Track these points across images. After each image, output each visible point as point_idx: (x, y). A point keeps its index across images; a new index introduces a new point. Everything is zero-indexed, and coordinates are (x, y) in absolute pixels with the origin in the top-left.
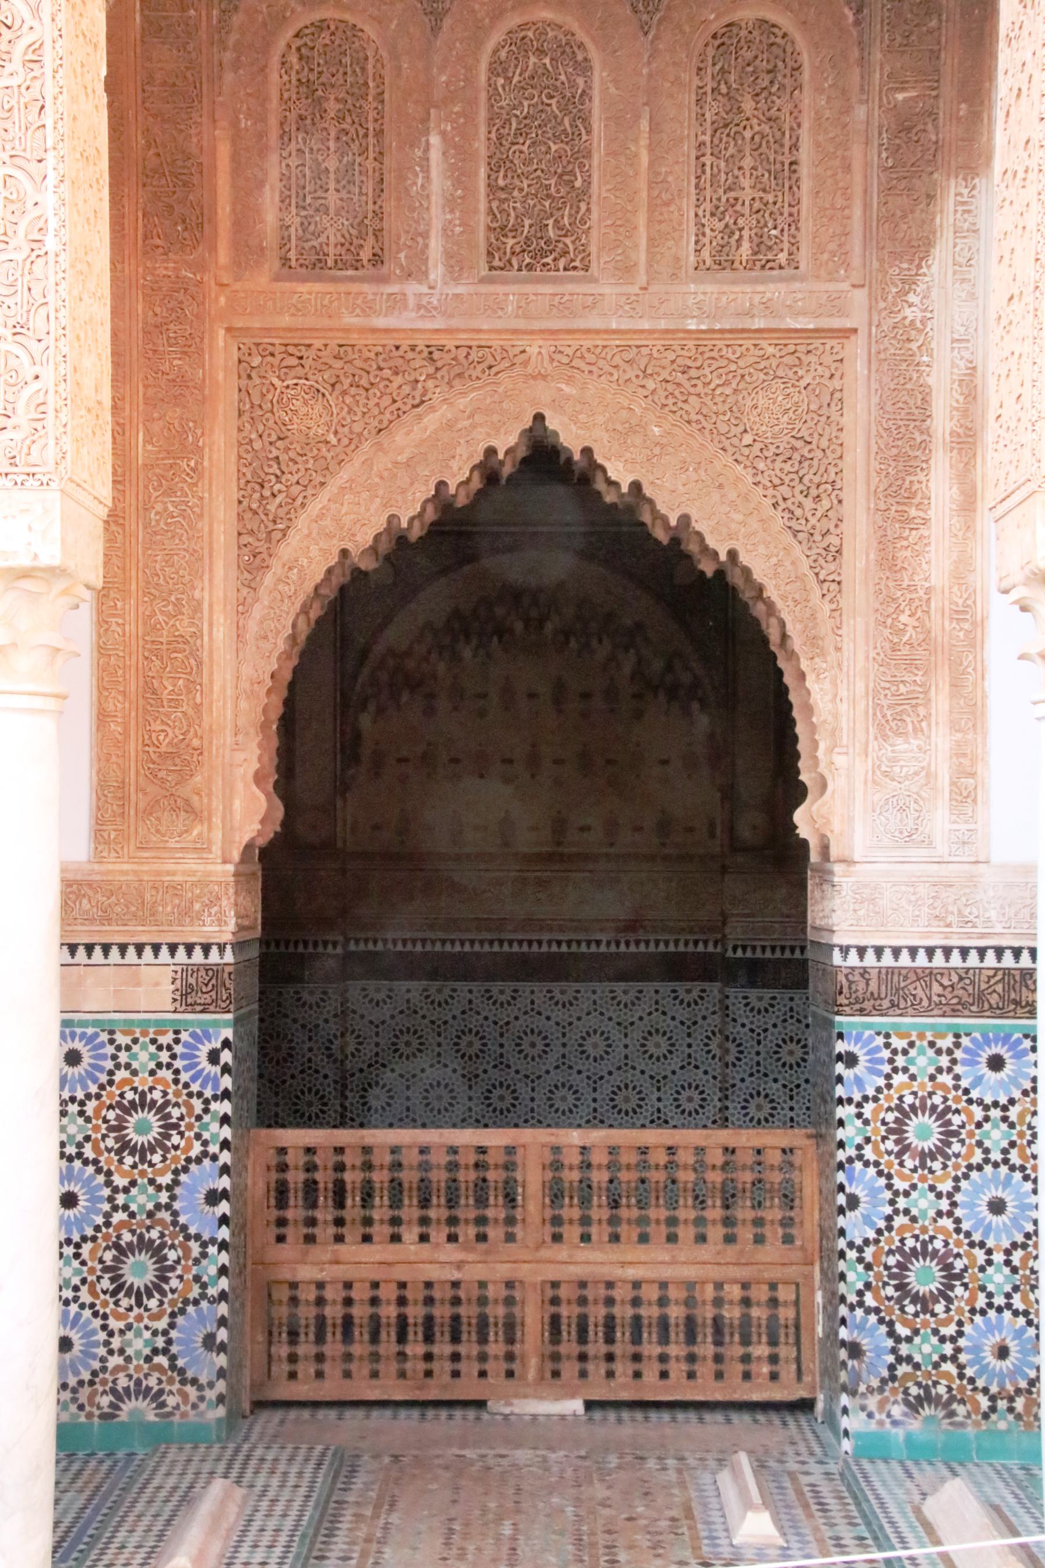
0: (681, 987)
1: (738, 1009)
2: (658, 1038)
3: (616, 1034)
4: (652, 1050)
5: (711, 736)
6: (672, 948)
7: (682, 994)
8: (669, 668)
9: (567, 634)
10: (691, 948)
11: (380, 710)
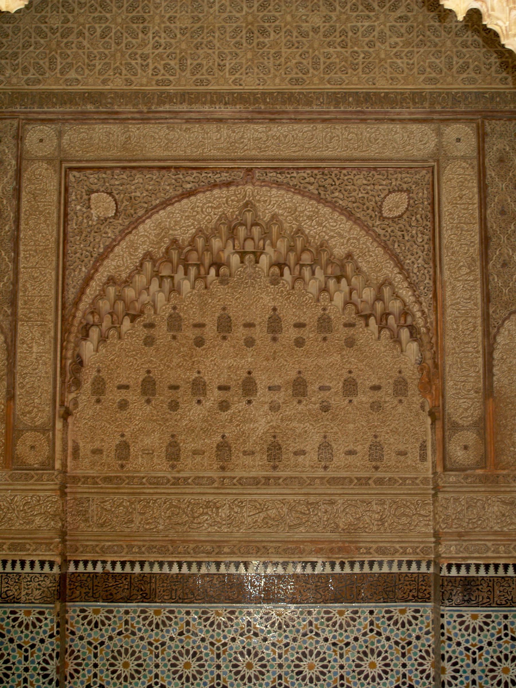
0: (395, 607)
1: (453, 629)
2: (372, 659)
3: (331, 655)
4: (367, 670)
5: (421, 363)
6: (385, 569)
7: (396, 615)
8: (379, 298)
9: (281, 266)
10: (404, 569)
11: (103, 339)
